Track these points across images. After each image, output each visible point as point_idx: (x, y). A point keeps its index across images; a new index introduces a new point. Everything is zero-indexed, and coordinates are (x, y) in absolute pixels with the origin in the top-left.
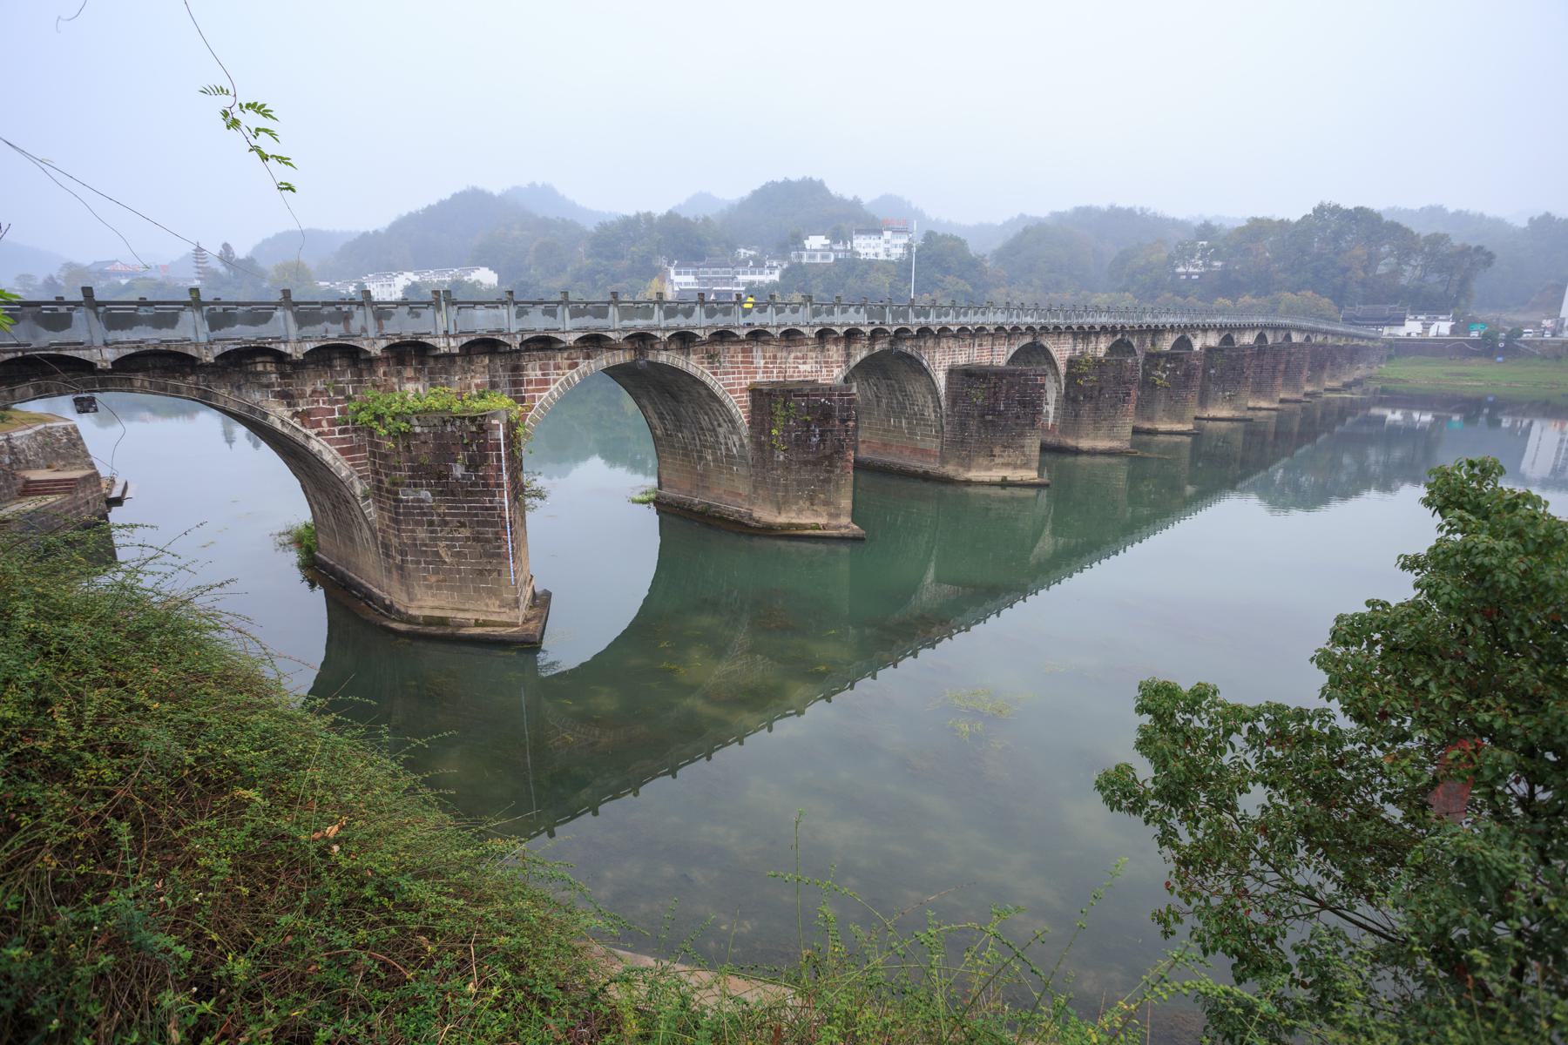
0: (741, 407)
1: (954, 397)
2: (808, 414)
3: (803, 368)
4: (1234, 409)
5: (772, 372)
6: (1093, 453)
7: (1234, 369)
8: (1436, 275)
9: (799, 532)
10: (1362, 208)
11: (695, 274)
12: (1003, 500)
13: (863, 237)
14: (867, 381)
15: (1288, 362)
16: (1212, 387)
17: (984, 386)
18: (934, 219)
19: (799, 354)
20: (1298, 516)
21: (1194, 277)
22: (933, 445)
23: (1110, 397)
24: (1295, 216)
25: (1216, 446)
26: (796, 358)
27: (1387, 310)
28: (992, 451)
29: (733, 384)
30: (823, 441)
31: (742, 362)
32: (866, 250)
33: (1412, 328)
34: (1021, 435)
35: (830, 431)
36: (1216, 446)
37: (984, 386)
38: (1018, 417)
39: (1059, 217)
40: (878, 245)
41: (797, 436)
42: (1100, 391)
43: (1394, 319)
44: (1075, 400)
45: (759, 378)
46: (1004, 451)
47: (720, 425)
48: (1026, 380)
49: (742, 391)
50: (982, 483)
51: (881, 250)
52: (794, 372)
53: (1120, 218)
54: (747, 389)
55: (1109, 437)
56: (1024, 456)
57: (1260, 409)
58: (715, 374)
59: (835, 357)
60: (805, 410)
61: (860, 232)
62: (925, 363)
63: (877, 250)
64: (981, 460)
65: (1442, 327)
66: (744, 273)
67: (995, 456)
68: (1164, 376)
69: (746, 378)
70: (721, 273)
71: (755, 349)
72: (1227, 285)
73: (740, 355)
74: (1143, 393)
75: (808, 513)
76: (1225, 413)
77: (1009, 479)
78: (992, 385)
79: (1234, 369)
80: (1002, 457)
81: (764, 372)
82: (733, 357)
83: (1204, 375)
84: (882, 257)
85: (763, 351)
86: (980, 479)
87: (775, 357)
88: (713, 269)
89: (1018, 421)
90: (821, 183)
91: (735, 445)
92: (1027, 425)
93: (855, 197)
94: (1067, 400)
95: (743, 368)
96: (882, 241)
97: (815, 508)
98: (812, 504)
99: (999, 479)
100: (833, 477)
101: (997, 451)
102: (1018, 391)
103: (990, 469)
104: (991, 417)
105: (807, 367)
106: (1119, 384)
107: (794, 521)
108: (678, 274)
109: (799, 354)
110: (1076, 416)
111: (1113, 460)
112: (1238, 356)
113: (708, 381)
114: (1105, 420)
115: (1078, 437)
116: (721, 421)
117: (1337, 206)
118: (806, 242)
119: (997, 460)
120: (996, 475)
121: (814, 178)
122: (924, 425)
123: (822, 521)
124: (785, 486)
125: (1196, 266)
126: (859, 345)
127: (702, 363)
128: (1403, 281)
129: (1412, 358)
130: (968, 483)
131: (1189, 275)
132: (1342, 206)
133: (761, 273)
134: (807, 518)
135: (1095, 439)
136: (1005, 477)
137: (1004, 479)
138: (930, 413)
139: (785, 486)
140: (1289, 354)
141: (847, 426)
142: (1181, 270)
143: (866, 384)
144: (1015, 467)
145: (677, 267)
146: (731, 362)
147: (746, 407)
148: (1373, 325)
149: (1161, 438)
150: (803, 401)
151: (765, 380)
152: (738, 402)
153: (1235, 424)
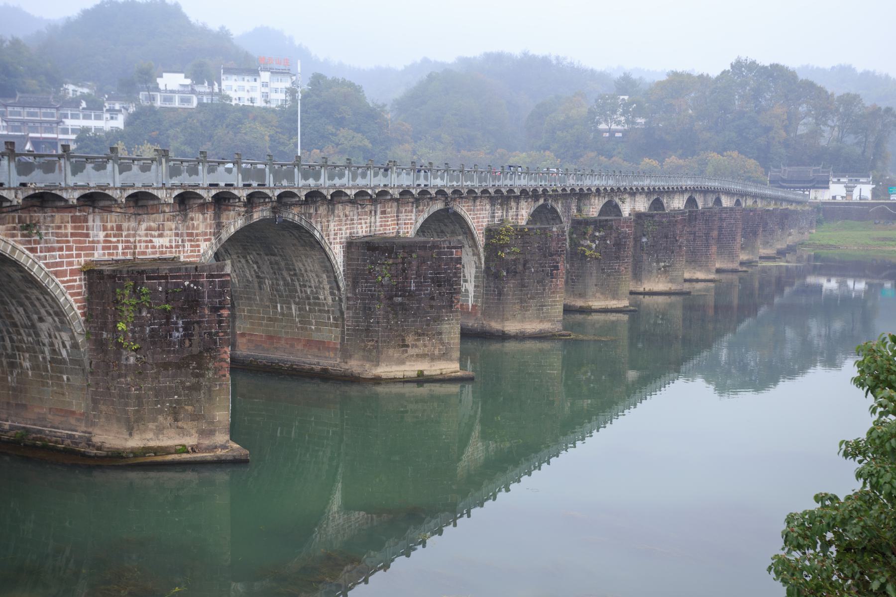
0: (72, 295)
1: (355, 276)
2: (167, 302)
3: (158, 242)
4: (671, 281)
5: (116, 248)
6: (521, 337)
7: (666, 237)
8: (852, 136)
9: (159, 459)
10: (777, 65)
12: (419, 400)
13: (234, 77)
14: (245, 257)
15: (720, 228)
16: (645, 257)
17: (391, 262)
18: (322, 60)
19: (152, 224)
20: (747, 398)
21: (617, 135)
22: (332, 335)
23: (537, 272)
24: (714, 72)
25: (655, 324)
26: (149, 229)
27: (811, 172)
28: (404, 340)
29: (61, 264)
30: (188, 335)
31: (73, 235)
32: (241, 94)
33: (836, 191)
34: (438, 319)
35: (198, 323)
36: (655, 324)
37: (391, 262)
38: (432, 298)
39: (465, 62)
40: (253, 89)
41: (152, 330)
42: (524, 265)
43: (818, 182)
44: (497, 276)
45: (98, 255)
46: (418, 340)
47: (41, 320)
48: (439, 254)
49: (73, 272)
50: (394, 381)
51: (257, 95)
52: (147, 247)
54: (80, 271)
55: (538, 317)
56: (443, 344)
57: (697, 281)
58: (33, 250)
60: (163, 296)
61: (229, 71)
62: (317, 235)
63: (253, 94)
65: (864, 191)
67: (408, 346)
68: (594, 246)
69: (78, 256)
70: (41, 115)
71: (90, 218)
73: (69, 225)
74: (572, 265)
75: (172, 432)
76: (661, 287)
77: (426, 373)
78: (400, 260)
79: (666, 237)
80: (416, 346)
81: (104, 248)
82: (59, 228)
83: (635, 246)
84: (259, 103)
85: (102, 220)
86: (392, 375)
87: (119, 228)
88: (27, 110)
89: (434, 303)
91: (64, 346)
92: (443, 307)
93: (222, 28)
94: (488, 275)
95: (75, 242)
96: (258, 84)
97: (180, 424)
98: (176, 420)
99: (414, 374)
100: (204, 382)
101: (410, 340)
102: (431, 267)
103: (402, 362)
104: (400, 299)
105: (165, 241)
106: (545, 257)
107: (152, 444)
109: (152, 224)
110: (500, 294)
111: (546, 345)
112: (669, 222)
113: (22, 260)
114: (532, 298)
115: (504, 319)
116: (43, 311)
117: (754, 63)
118: (159, 80)
119: (411, 351)
120: (410, 369)
122: (320, 311)
123: (190, 441)
124: (138, 397)
125: (618, 123)
126: (232, 213)
127: (13, 236)
128: (823, 142)
129: (839, 223)
130: (377, 380)
131: (612, 132)
132: (758, 62)
133: (98, 118)
134: (169, 438)
135: (523, 320)
136: (422, 372)
137: (421, 373)
138: (326, 297)
139: (138, 397)
140: (721, 219)
141: (220, 316)
142: (603, 126)
143: (243, 261)
144: (433, 358)
146: (57, 235)
147: (79, 294)
148: (800, 188)
149: (595, 317)
150: (160, 284)
151: (106, 258)
152: (68, 288)
153: (673, 298)
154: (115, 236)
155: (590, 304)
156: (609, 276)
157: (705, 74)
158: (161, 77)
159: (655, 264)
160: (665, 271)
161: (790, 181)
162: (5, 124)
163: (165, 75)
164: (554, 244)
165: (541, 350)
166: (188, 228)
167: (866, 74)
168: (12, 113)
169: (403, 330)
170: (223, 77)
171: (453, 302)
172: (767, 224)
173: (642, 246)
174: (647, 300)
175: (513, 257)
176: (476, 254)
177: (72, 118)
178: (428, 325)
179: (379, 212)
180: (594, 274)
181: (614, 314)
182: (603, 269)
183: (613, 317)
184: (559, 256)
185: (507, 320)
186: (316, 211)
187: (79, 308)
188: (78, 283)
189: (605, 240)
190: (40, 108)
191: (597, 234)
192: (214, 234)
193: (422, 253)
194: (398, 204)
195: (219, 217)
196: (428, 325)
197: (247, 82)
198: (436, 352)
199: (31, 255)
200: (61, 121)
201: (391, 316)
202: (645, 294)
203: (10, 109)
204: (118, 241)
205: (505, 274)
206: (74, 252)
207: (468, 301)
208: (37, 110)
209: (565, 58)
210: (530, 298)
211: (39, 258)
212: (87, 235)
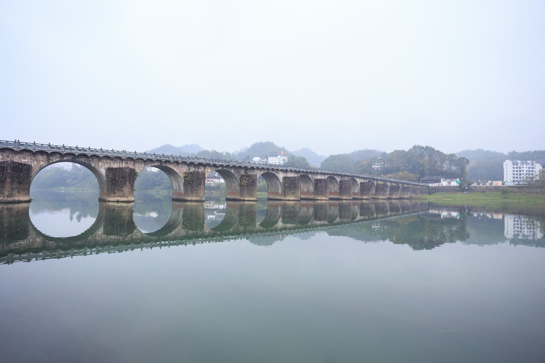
1: (107, 176)
3: (23, 160)
4: (295, 197)
6: (191, 201)
8: (455, 167)
10: (427, 146)
12: (118, 207)
13: (271, 157)
15: (345, 186)
17: (112, 172)
25: (290, 209)
27: (435, 178)
28: (115, 192)
30: (3, 176)
32: (273, 161)
33: (444, 183)
34: (122, 187)
36: (290, 209)
37: (112, 172)
38: (121, 182)
40: (276, 160)
42: (192, 182)
43: (437, 181)
46: (118, 192)
50: (112, 201)
53: (368, 152)
56: (123, 193)
57: (323, 200)
59: (41, 159)
61: (270, 156)
62: (93, 166)
63: (276, 161)
64: (112, 195)
65: (454, 183)
67: (115, 193)
72: (386, 171)
74: (241, 188)
76: (292, 198)
77: (119, 200)
80: (117, 193)
81: (1, 160)
83: (284, 186)
84: (277, 164)
86: (111, 200)
89: (122, 183)
90: (273, 143)
92: (124, 184)
93: (283, 147)
96: (277, 159)
99: (116, 200)
101: (116, 192)
102: (121, 174)
103: (114, 197)
105: (26, 160)
111: (198, 204)
114: (194, 191)
117: (420, 146)
118: (253, 159)
119: (116, 195)
120: (116, 199)
121: (271, 141)
125: (378, 165)
126: (54, 157)
129: (440, 193)
130: (109, 201)
131: (377, 168)
135: (192, 197)
137: (118, 200)
140: (346, 184)
142: (373, 167)
144: (121, 197)
149: (246, 202)
153: (296, 202)
154: (6, 157)
155: (245, 199)
156: (250, 191)
157: (404, 150)
159: (290, 192)
160: (293, 194)
161: (427, 181)
163: (255, 157)
164: (200, 176)
165: (197, 205)
166: (36, 158)
167: (487, 151)
169: (115, 189)
170: (269, 157)
171: (126, 183)
172: (383, 188)
173: (286, 187)
174: (288, 202)
175: (189, 180)
176: (181, 179)
178: (120, 188)
179: (124, 163)
180: (246, 190)
181: (252, 202)
182: (249, 189)
183: (252, 203)
184: (202, 179)
185: (188, 196)
186: (92, 160)
189: (249, 181)
191: (247, 179)
192: (47, 161)
193: (119, 170)
194: (134, 162)
195: (49, 157)
196: (120, 188)
197: (274, 158)
198: (122, 195)
201: (112, 186)
202: (287, 200)
205: (187, 184)
209: (378, 150)
210: (194, 191)
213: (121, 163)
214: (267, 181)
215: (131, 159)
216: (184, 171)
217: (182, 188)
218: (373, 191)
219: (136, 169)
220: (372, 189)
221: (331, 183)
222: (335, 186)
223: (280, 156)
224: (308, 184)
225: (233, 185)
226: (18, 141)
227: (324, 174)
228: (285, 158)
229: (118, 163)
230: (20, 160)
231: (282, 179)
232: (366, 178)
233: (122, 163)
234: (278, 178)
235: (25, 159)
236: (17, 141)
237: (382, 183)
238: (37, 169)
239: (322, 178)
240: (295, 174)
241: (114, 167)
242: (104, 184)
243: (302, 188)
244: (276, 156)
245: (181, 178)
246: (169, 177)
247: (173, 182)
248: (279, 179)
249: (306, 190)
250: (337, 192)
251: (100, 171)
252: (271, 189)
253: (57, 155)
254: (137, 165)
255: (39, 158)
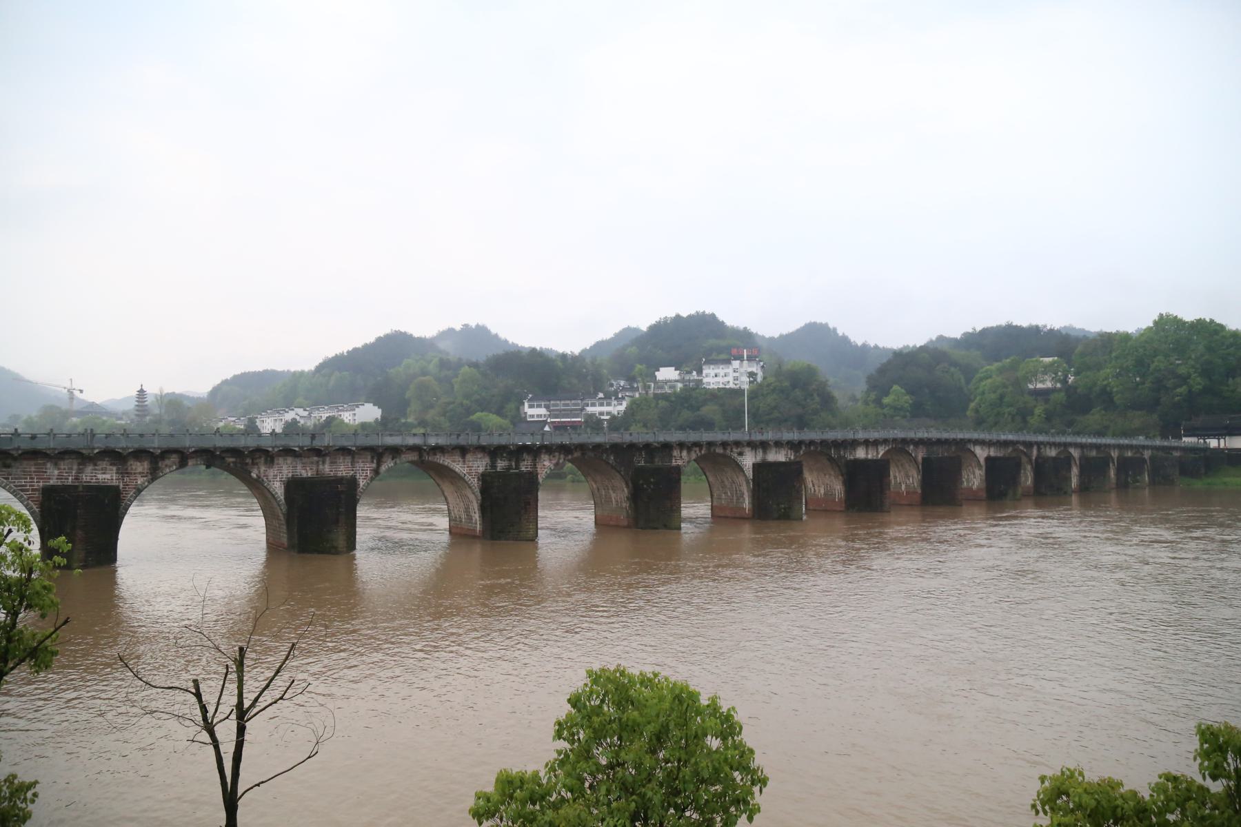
3: (100, 476)
5: (68, 479)
11: (547, 407)
13: (712, 367)
29: (26, 486)
31: (34, 472)
51: (730, 378)
61: (709, 362)
66: (593, 405)
70: (571, 404)
88: (563, 402)
90: (713, 316)
105: (108, 476)
108: (531, 406)
132: (1179, 317)
133: (609, 404)
145: (530, 400)
146: (24, 472)
151: (59, 484)
154: (66, 473)
158: (658, 370)
162: (548, 413)
163: (661, 369)
168: (554, 405)
170: (704, 367)
176: (474, 493)
177: (607, 406)
187: (37, 508)
188: (37, 495)
190: (571, 400)
194: (353, 458)
197: (721, 370)
199: (5, 481)
200: (584, 409)
203: (552, 402)
204: (69, 476)
206: (35, 480)
207: (476, 527)
208: (569, 402)
209: (1045, 326)
211: (11, 482)
212: (46, 472)
213: (321, 463)
214: (708, 474)
215: (344, 451)
216: (481, 470)
217: (477, 516)
218: (1027, 480)
219: (358, 477)
220: (1025, 473)
221: (897, 466)
222: (910, 474)
223: (738, 362)
224: (827, 476)
225: (613, 495)
226: (92, 430)
227: (876, 443)
228: (755, 368)
229: (312, 463)
230: (95, 476)
231: (751, 470)
232: (1006, 444)
233: (324, 463)
234: (739, 468)
235: (104, 473)
236: (89, 431)
237: (1052, 453)
238: (131, 497)
239: (870, 457)
240: (789, 451)
241: (305, 475)
242: (280, 520)
243: (810, 485)
244: (727, 362)
245: (472, 490)
246: (439, 485)
247: (449, 499)
248: (744, 472)
249: (822, 491)
250: (917, 492)
251: (271, 490)
252: (720, 499)
253: (174, 456)
254: (360, 465)
255: (134, 467)
